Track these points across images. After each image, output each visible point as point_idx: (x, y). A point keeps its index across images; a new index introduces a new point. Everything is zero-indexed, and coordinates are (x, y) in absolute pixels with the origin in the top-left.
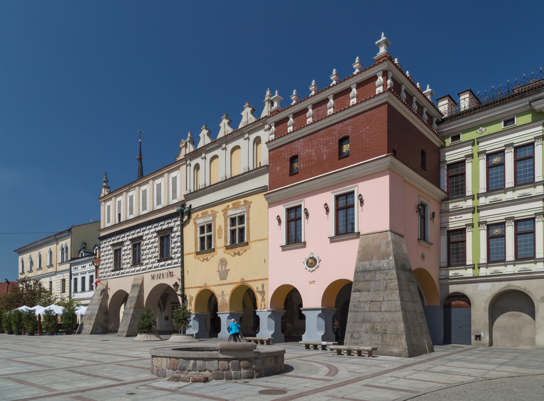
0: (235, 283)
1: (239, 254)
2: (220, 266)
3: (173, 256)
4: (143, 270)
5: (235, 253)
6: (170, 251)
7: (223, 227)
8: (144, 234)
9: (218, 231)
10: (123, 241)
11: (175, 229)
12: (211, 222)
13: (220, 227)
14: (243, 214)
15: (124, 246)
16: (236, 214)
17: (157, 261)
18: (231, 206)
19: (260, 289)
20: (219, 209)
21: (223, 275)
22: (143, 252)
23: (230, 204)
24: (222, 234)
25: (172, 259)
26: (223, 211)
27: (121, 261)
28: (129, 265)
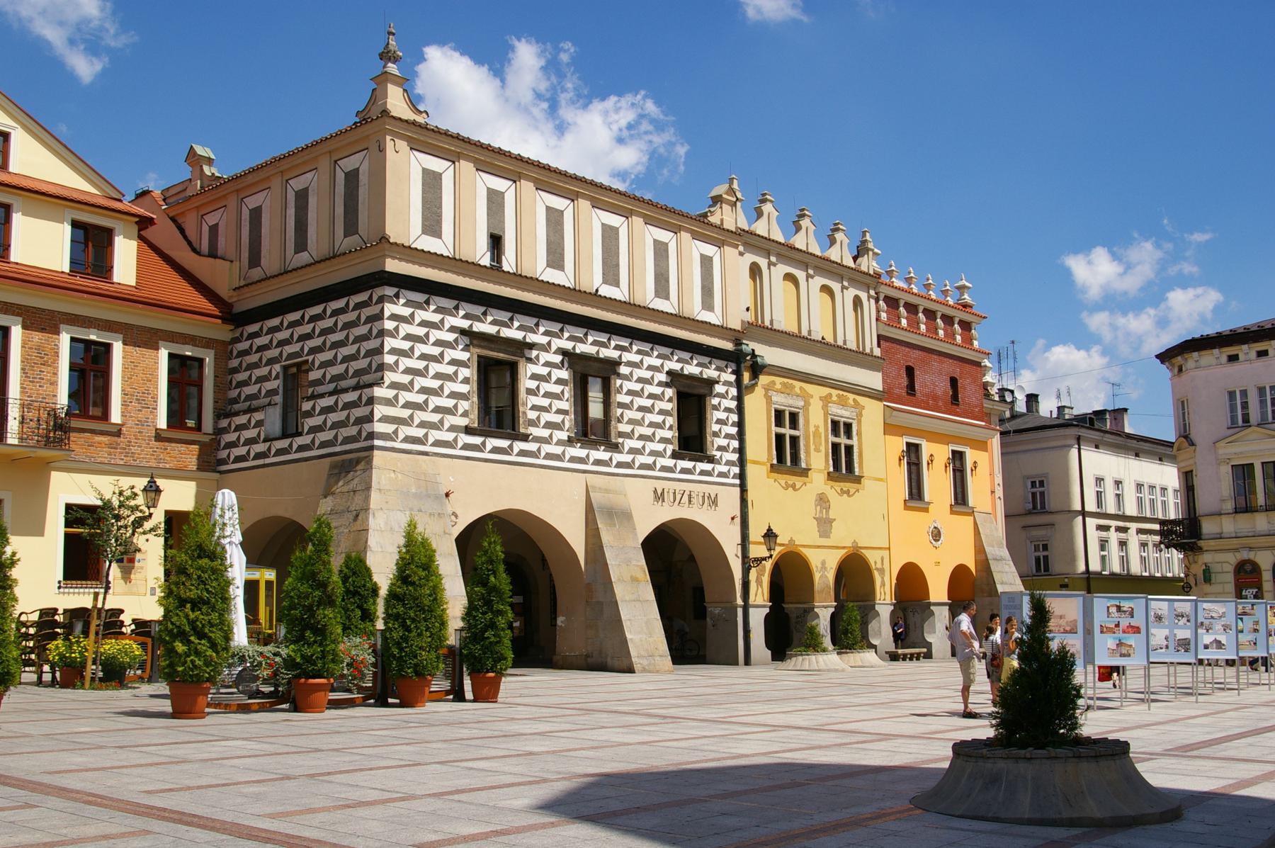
0: (844, 548)
1: (848, 492)
2: (818, 508)
3: (718, 454)
4: (620, 465)
5: (842, 489)
6: (709, 439)
7: (822, 430)
8: (624, 359)
9: (814, 437)
10: (528, 340)
11: (719, 389)
12: (798, 410)
13: (817, 427)
14: (850, 421)
15: (530, 360)
16: (842, 417)
17: (669, 453)
18: (834, 398)
19: (879, 566)
20: (816, 391)
21: (825, 525)
22: (619, 411)
23: (834, 392)
24: (821, 444)
25: (711, 460)
26: (821, 398)
27: (521, 409)
28: (563, 435)
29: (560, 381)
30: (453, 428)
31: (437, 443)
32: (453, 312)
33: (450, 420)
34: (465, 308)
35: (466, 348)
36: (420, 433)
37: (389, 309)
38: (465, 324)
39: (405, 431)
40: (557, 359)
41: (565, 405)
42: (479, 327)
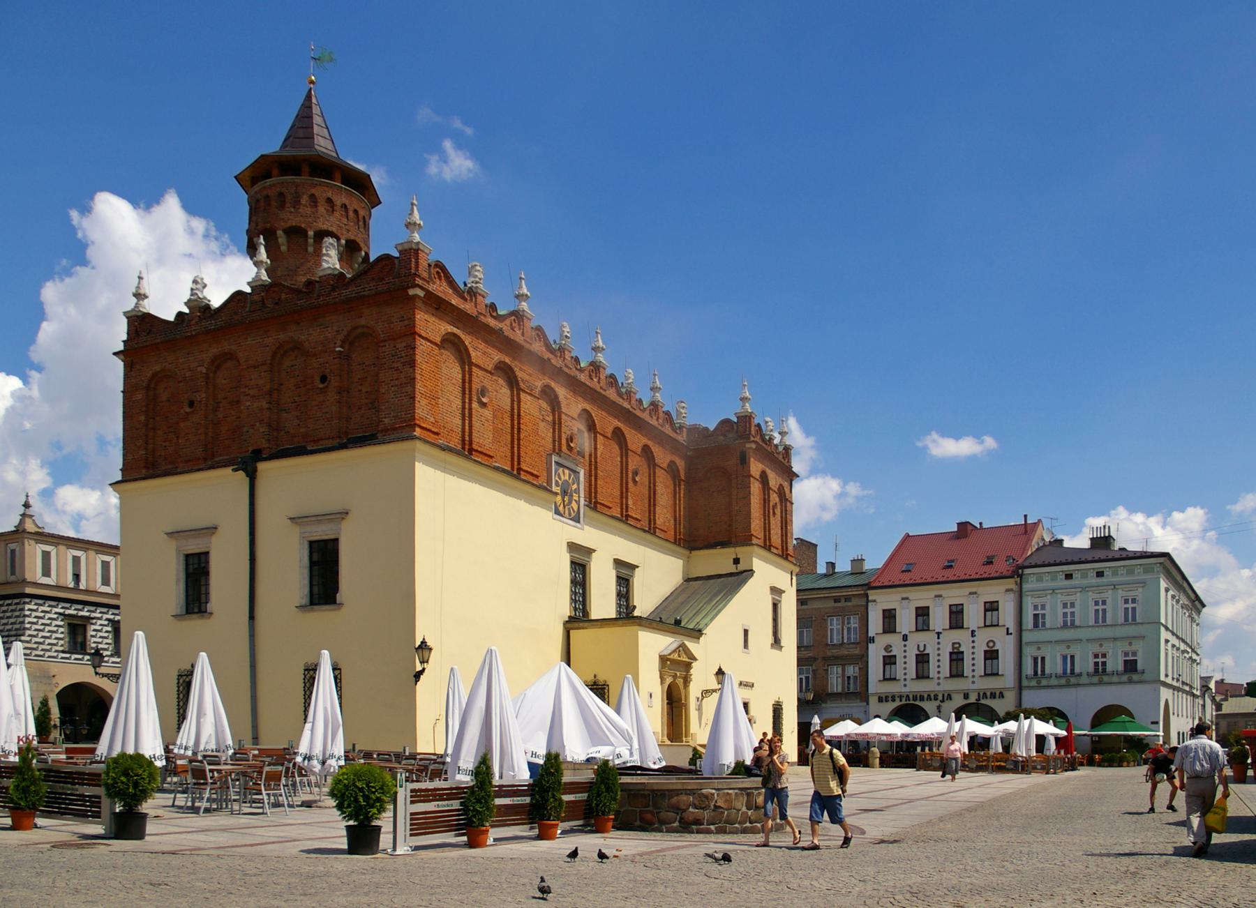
15: (92, 624)
28: (109, 653)
29: (107, 632)
30: (56, 651)
31: (49, 657)
32: (56, 607)
33: (55, 648)
34: (62, 605)
35: (62, 621)
36: (42, 653)
37: (27, 607)
38: (62, 611)
39: (35, 653)
40: (106, 623)
41: (109, 641)
42: (68, 612)
